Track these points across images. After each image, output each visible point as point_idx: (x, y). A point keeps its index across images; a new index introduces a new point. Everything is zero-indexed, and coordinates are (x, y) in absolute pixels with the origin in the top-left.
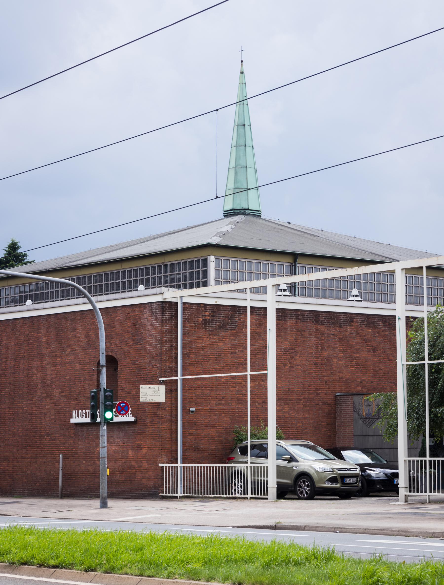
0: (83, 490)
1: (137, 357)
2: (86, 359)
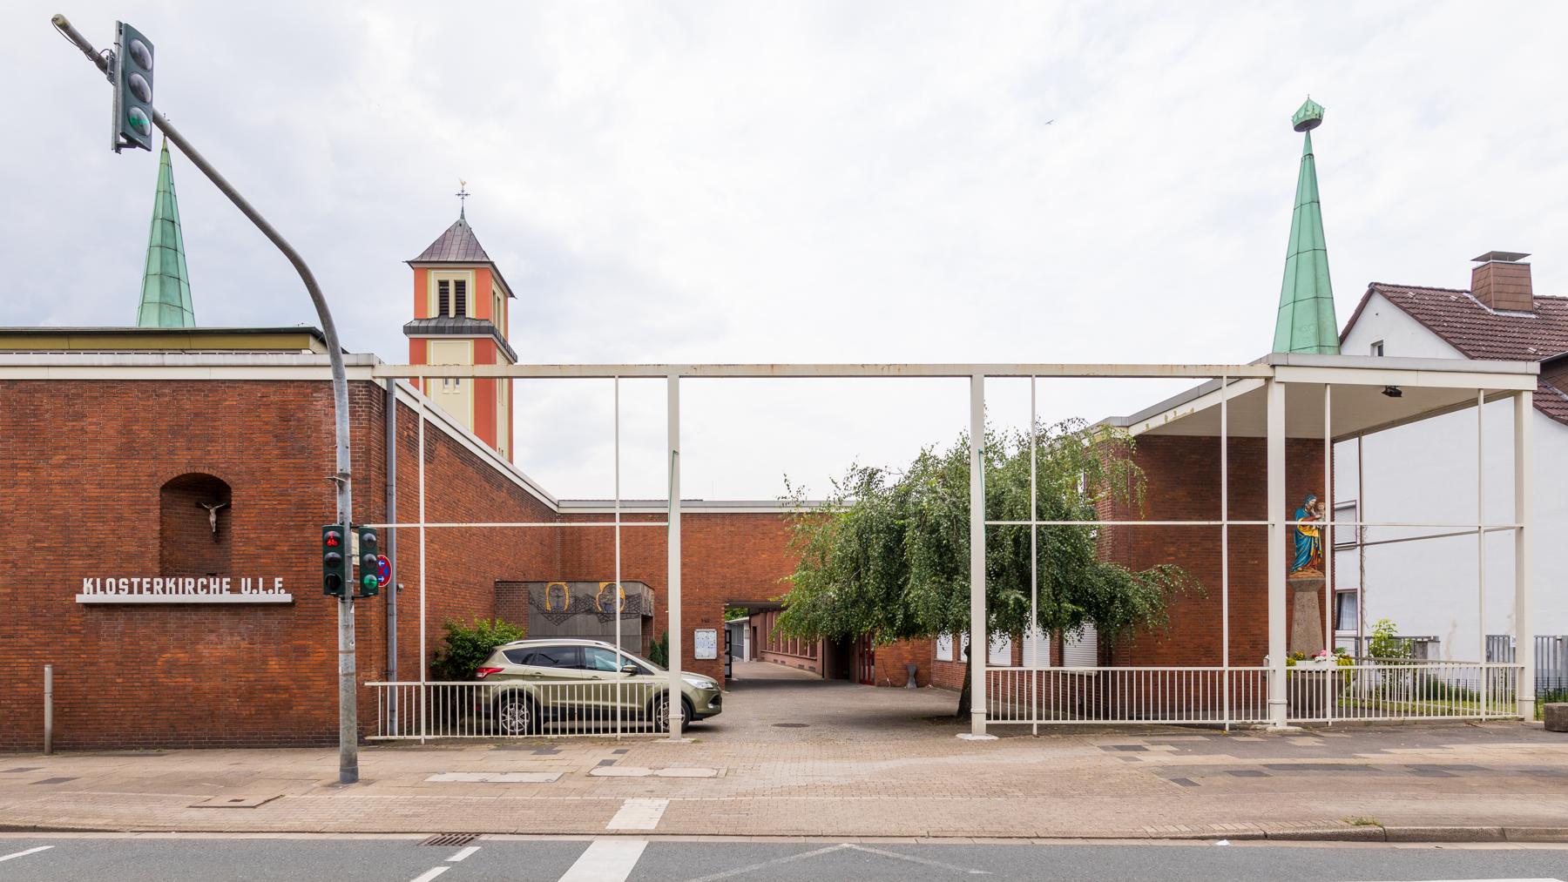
0: (117, 735)
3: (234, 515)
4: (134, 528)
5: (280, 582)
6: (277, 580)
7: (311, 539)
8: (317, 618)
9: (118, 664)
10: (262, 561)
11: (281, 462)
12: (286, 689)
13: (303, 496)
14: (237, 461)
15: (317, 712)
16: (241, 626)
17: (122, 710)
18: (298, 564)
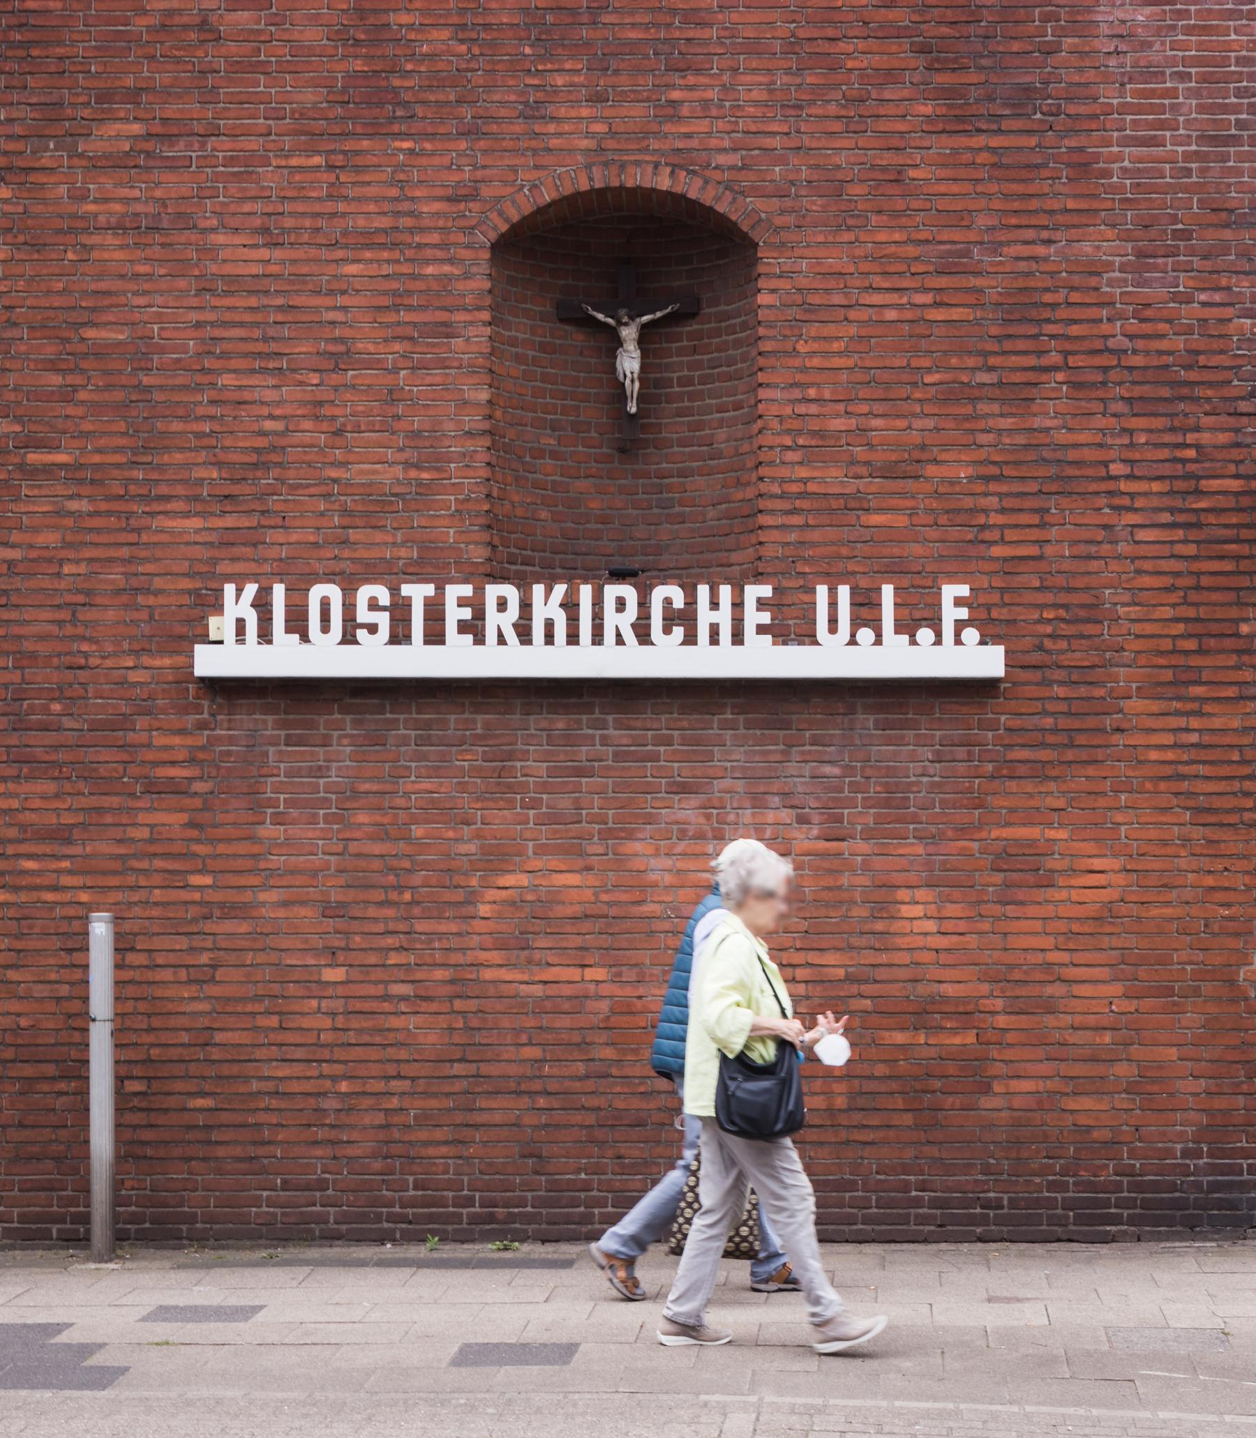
0: (322, 1185)
1: (982, 221)
2: (341, 207)
3: (767, 346)
4: (393, 395)
5: (959, 602)
6: (950, 592)
7: (1062, 437)
8: (1081, 739)
9: (330, 910)
10: (876, 519)
11: (942, 145)
12: (965, 1014)
13: (1030, 274)
14: (776, 142)
15: (1086, 1103)
16: (792, 768)
17: (344, 1087)
18: (1010, 535)
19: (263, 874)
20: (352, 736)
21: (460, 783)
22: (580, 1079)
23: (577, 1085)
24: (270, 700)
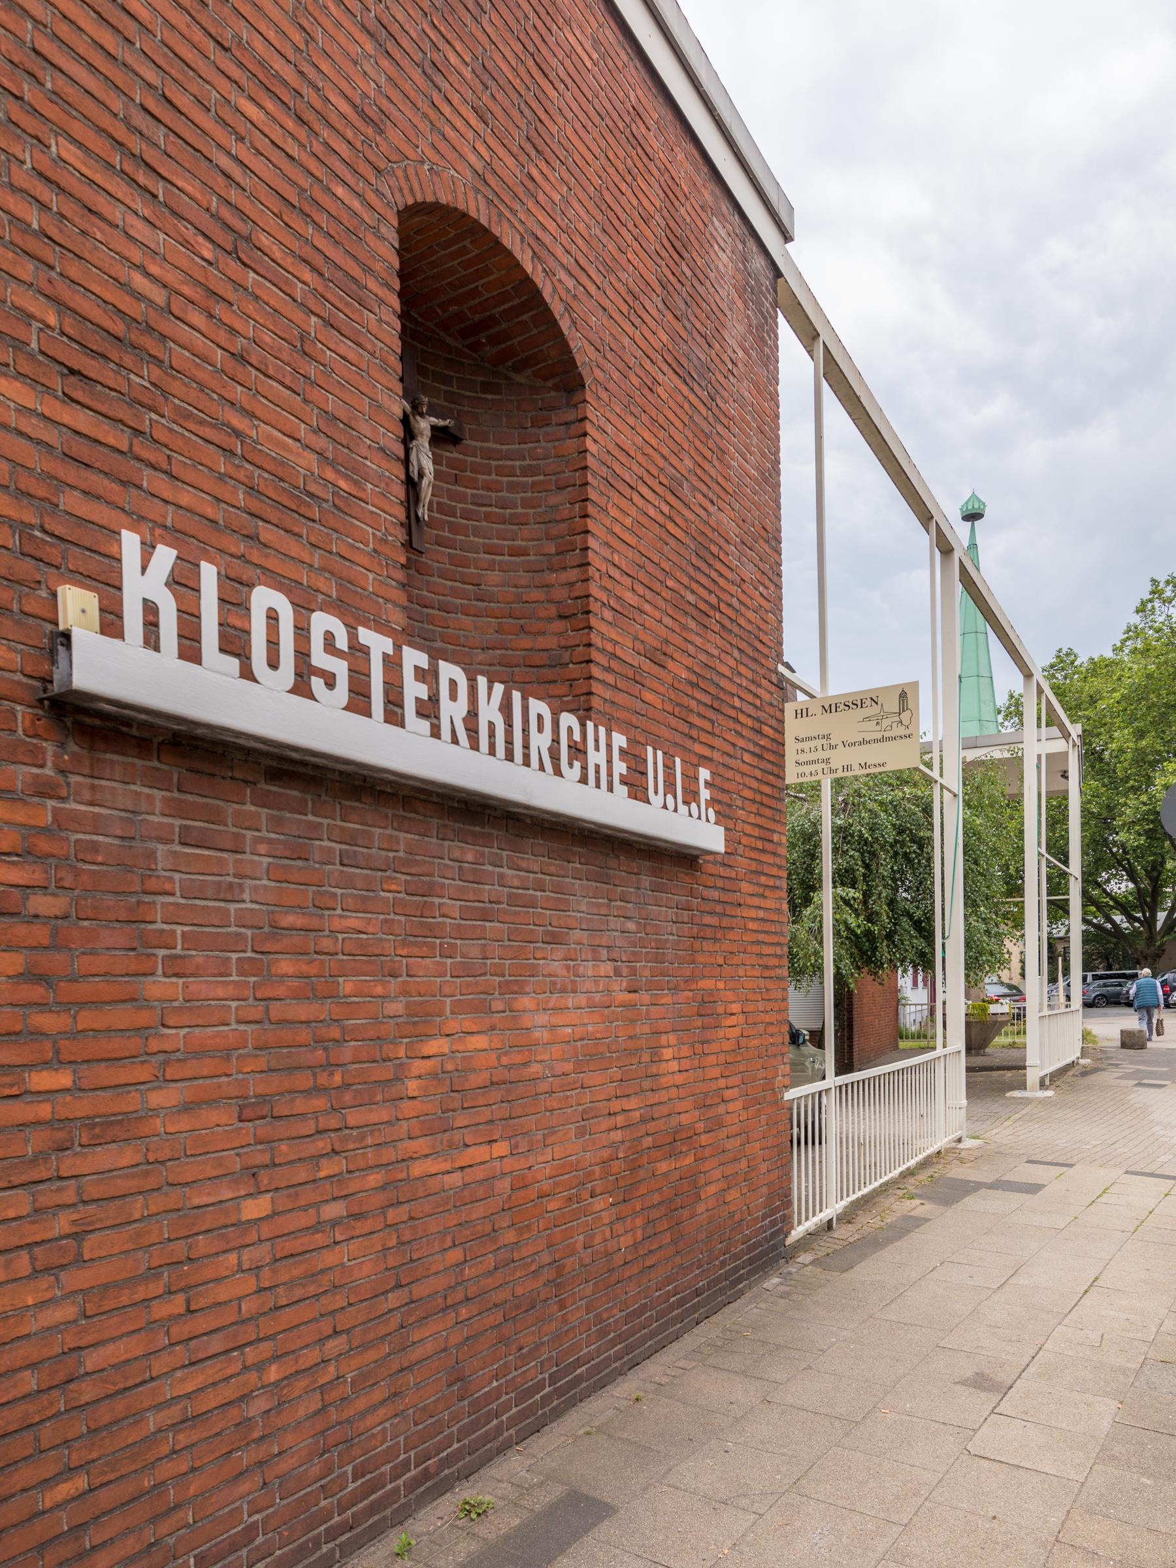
19: (153, 1059)
20: (270, 842)
21: (386, 921)
22: (490, 1273)
23: (489, 1282)
24: (156, 764)
